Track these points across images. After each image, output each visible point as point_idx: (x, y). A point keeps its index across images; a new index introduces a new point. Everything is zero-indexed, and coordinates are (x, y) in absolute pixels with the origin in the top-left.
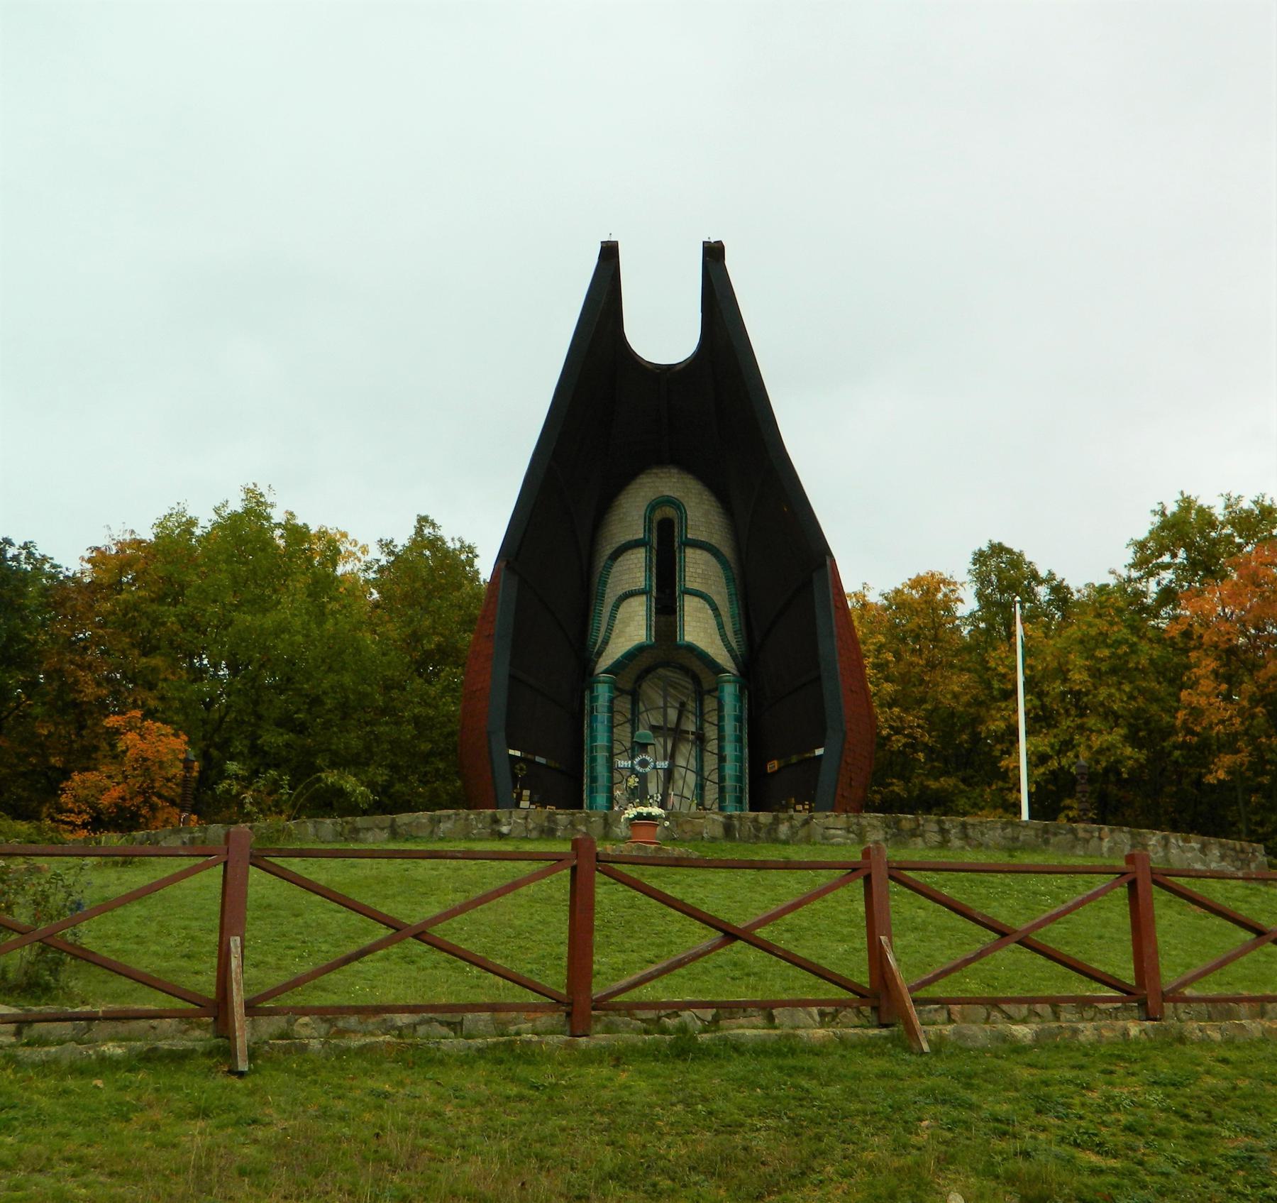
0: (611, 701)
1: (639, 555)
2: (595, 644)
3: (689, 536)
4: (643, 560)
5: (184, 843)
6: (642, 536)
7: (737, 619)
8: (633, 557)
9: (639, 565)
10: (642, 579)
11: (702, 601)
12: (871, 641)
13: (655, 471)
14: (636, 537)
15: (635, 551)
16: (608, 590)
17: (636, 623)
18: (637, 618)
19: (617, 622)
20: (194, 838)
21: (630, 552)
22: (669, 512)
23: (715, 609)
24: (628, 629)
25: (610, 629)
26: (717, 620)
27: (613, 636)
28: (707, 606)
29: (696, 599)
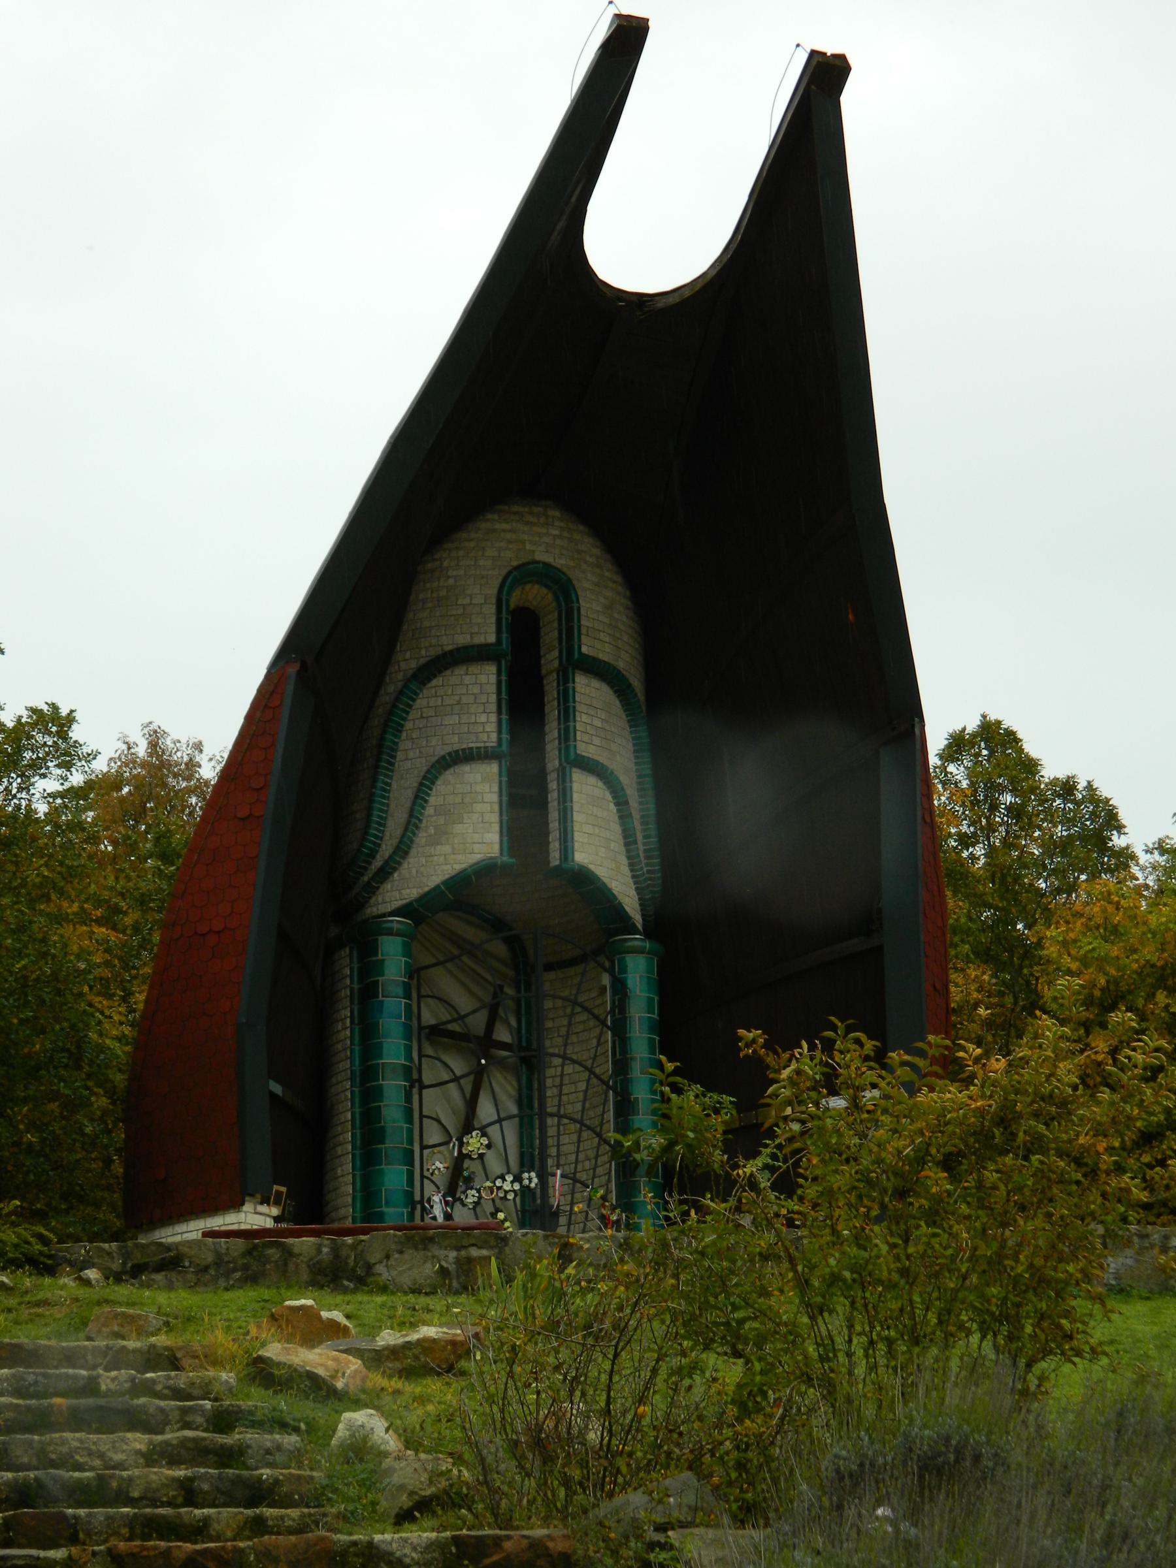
0: (414, 973)
1: (483, 678)
2: (372, 855)
3: (584, 649)
4: (493, 689)
5: (444, 1272)
6: (492, 639)
7: (652, 826)
8: (467, 679)
9: (484, 699)
10: (492, 727)
11: (600, 784)
12: (505, 859)
13: (515, 508)
14: (479, 640)
15: (474, 669)
16: (404, 745)
17: (475, 817)
18: (478, 807)
19: (430, 811)
20: (470, 1260)
21: (460, 670)
22: (535, 595)
23: (621, 802)
24: (458, 828)
25: (413, 821)
26: (623, 824)
27: (421, 838)
28: (609, 797)
29: (592, 780)
